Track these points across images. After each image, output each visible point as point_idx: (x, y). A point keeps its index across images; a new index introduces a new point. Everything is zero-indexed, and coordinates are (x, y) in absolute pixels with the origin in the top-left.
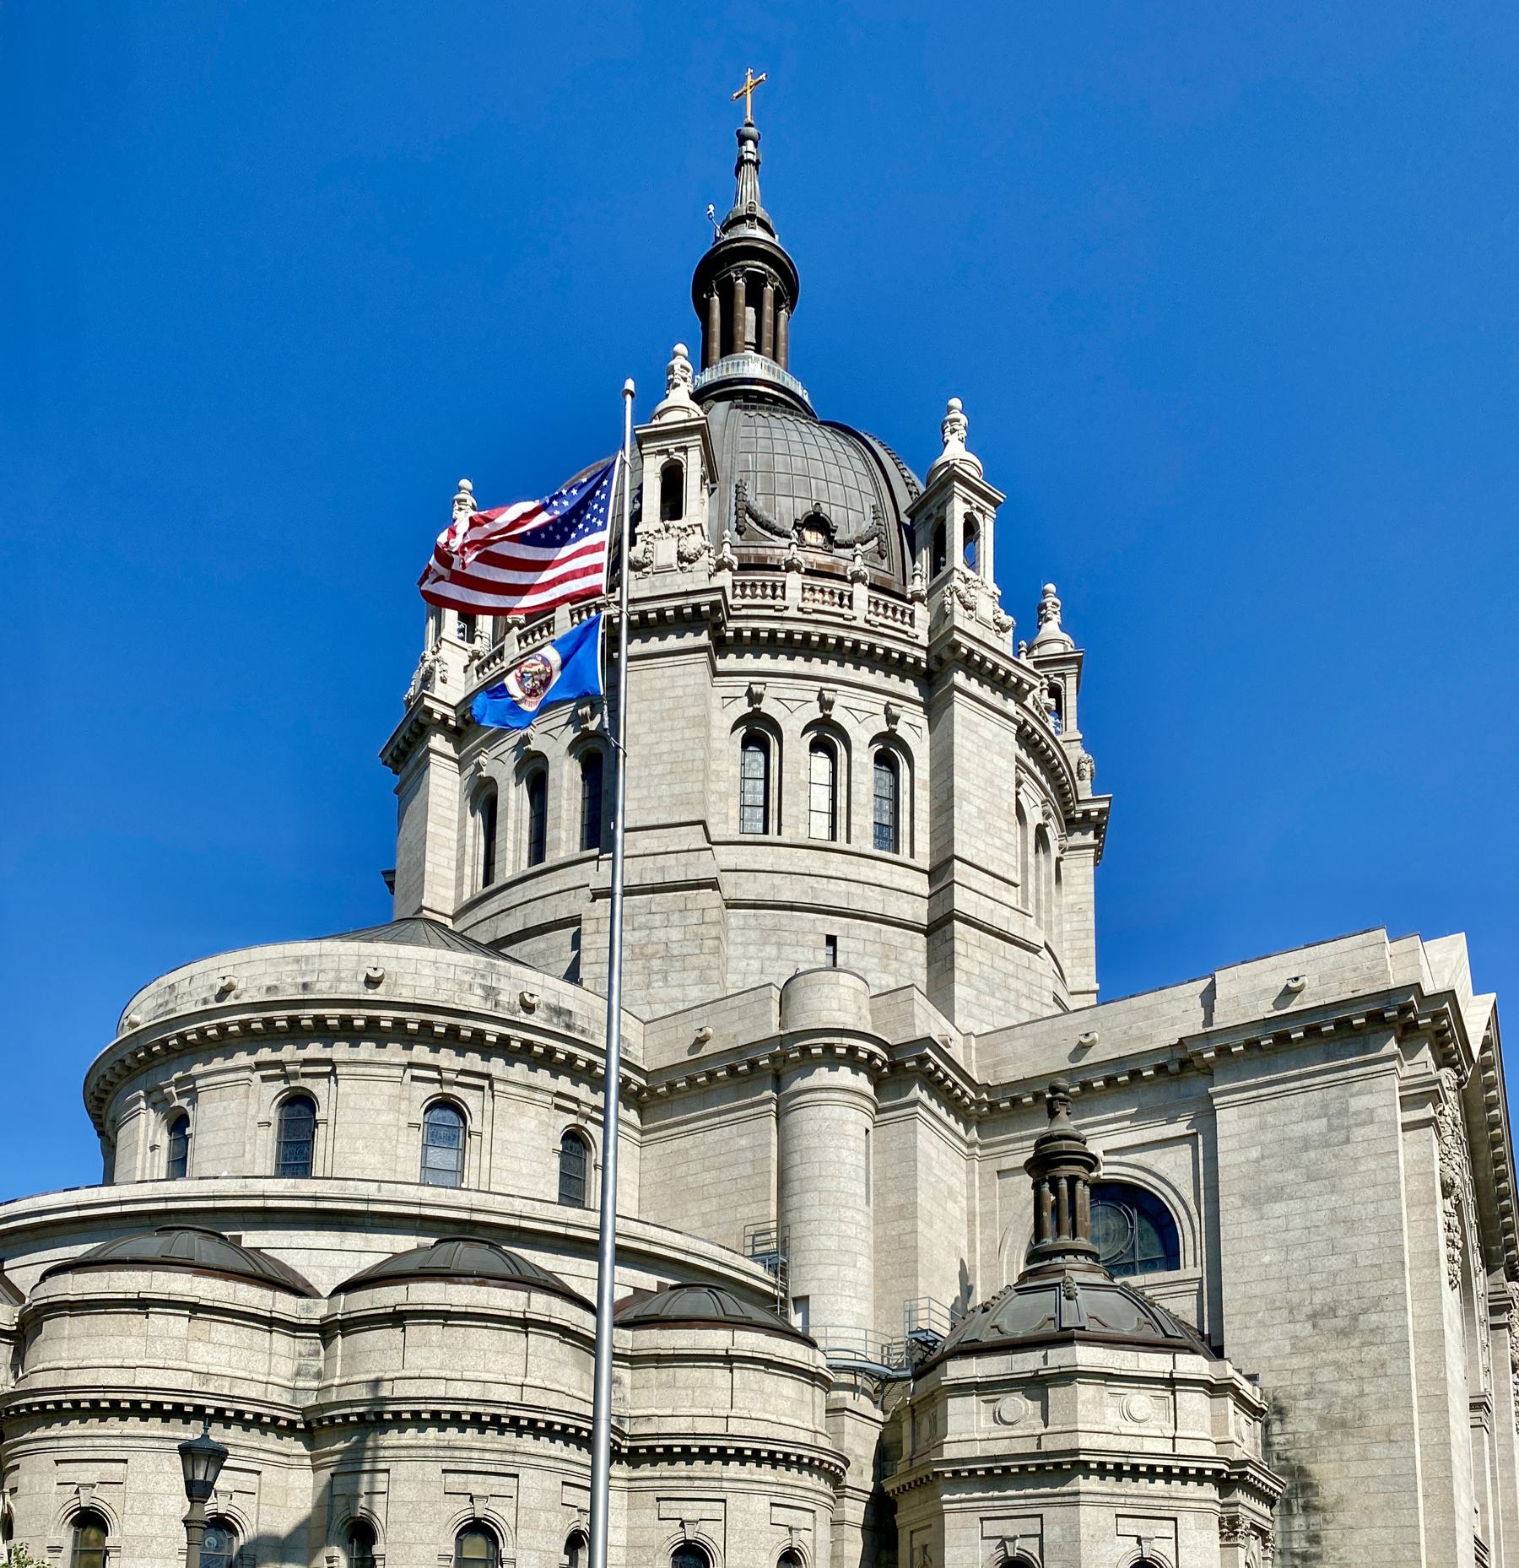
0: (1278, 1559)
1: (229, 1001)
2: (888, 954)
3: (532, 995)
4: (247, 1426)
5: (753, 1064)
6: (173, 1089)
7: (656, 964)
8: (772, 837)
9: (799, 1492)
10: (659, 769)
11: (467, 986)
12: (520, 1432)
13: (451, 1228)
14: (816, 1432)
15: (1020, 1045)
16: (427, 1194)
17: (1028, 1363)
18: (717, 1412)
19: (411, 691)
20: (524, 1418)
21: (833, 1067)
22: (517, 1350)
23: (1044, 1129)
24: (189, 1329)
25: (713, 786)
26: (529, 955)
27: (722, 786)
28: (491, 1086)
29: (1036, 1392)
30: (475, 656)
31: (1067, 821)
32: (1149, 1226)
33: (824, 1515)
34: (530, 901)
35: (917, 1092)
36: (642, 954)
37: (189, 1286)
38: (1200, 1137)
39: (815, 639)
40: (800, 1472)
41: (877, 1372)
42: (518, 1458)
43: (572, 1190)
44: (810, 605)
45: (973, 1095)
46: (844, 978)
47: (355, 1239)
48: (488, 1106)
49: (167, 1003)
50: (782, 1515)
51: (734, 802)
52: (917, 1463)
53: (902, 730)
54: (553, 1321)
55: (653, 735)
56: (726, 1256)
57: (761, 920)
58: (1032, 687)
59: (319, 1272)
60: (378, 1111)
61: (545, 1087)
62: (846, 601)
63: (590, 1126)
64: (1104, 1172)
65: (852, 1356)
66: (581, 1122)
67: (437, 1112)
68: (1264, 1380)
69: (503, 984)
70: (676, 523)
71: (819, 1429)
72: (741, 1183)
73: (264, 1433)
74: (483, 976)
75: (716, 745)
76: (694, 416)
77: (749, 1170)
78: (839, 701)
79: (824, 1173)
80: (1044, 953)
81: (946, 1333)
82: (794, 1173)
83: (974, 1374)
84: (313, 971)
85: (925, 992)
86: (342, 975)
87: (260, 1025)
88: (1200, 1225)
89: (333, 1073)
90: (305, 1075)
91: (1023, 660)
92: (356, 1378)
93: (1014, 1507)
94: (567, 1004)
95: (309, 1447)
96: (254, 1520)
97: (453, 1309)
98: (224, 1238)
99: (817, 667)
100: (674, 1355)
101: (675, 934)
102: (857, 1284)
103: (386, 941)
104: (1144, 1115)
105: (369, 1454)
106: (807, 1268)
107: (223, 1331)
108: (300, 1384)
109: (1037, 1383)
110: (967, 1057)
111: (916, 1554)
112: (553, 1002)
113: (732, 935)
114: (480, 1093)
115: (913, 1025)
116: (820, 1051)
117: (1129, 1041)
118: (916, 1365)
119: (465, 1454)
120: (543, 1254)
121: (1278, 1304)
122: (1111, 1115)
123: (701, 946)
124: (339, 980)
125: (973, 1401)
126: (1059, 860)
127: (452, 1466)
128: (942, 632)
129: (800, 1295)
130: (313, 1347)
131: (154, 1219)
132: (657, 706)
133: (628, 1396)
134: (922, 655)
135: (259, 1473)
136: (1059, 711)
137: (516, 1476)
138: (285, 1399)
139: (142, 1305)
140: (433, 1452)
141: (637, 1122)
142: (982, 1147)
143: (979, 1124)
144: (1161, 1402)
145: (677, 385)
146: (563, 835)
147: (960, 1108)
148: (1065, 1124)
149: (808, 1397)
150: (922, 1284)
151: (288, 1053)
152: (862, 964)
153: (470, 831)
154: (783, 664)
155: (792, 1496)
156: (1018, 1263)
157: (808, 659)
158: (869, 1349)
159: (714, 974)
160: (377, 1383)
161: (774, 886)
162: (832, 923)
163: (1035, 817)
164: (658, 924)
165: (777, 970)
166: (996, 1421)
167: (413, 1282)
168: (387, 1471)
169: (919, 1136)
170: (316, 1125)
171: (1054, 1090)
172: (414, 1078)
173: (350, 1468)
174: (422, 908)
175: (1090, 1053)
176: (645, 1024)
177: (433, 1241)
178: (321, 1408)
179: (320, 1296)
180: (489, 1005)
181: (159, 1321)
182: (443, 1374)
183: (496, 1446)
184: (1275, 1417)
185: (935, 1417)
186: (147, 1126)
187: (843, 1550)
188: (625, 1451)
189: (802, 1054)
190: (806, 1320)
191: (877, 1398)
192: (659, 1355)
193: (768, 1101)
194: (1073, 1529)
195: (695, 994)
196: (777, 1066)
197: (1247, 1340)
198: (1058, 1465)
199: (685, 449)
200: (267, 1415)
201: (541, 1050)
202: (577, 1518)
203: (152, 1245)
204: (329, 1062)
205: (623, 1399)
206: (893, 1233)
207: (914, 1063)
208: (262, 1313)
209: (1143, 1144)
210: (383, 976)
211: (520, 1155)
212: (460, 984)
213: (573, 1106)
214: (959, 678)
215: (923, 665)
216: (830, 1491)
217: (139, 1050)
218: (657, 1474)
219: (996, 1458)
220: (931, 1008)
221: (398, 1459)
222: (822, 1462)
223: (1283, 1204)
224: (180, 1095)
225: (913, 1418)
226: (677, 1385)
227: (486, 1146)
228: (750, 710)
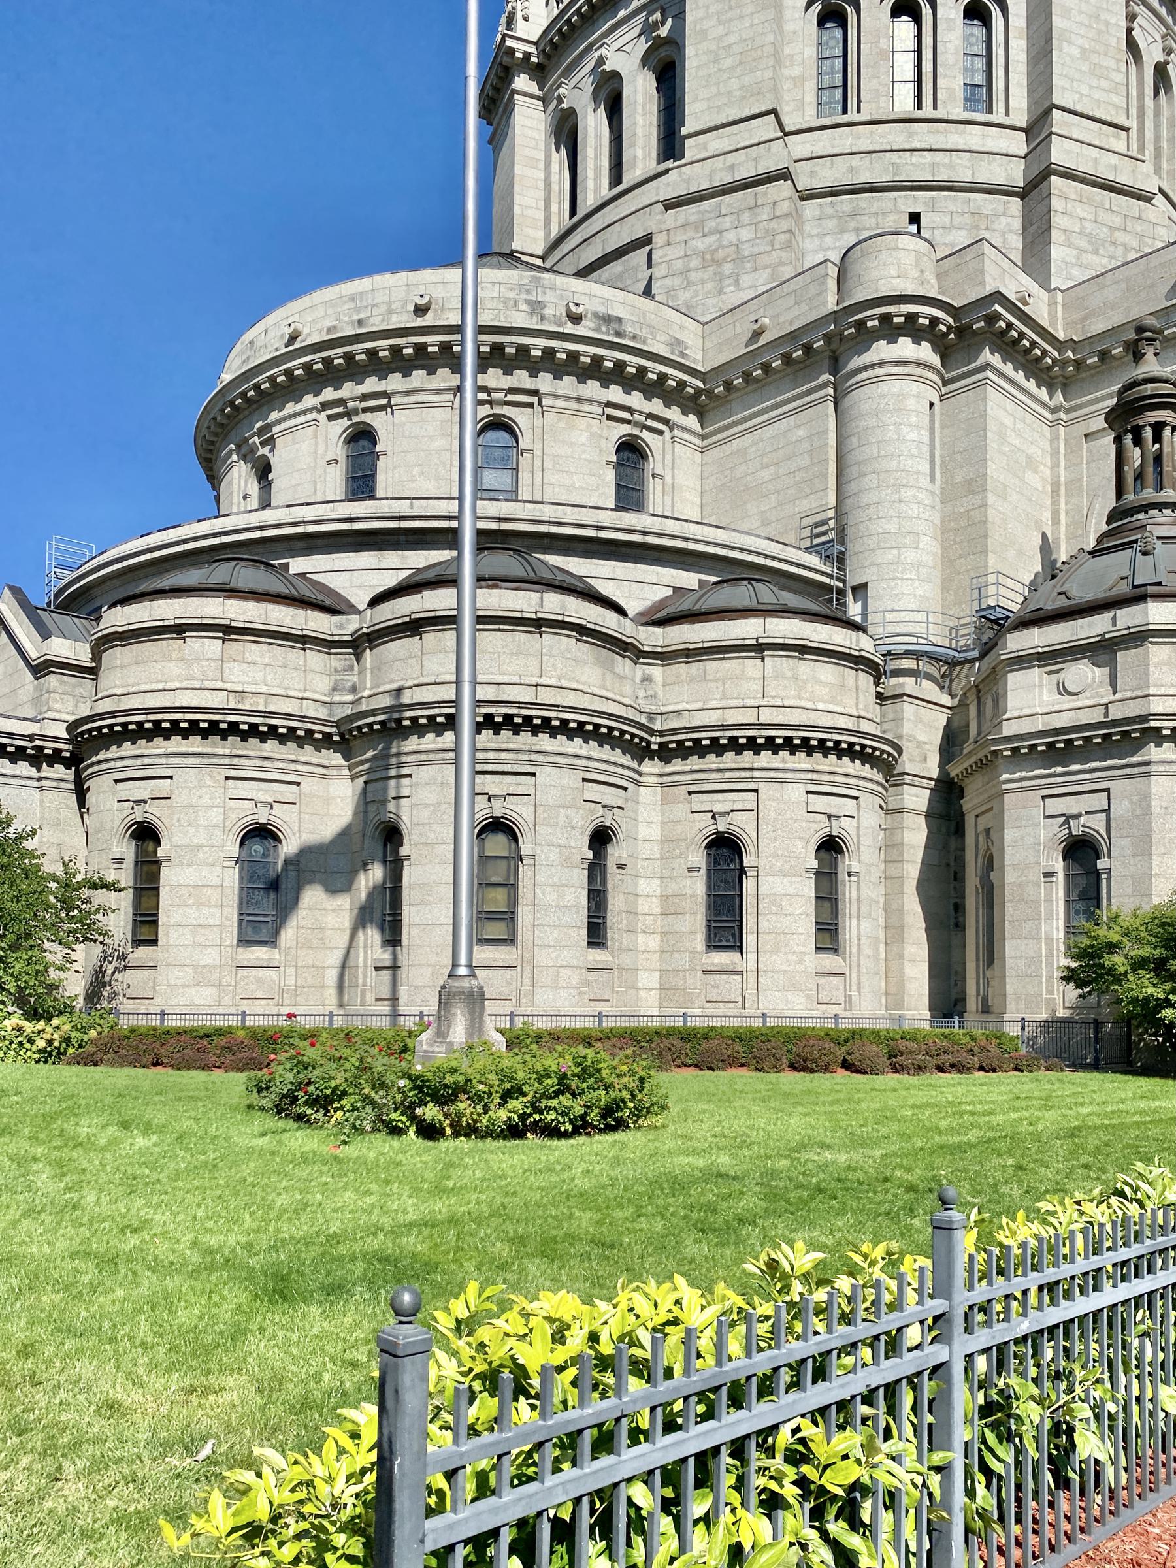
3: (577, 305)
4: (283, 740)
5: (808, 348)
7: (727, 268)
12: (535, 731)
14: (859, 717)
15: (1111, 293)
18: (749, 703)
20: (537, 717)
21: (892, 340)
25: (786, 72)
34: (609, 226)
35: (987, 356)
36: (713, 260)
41: (942, 654)
45: (1056, 354)
50: (819, 803)
51: (811, 86)
55: (721, 27)
56: (774, 549)
66: (636, 432)
72: (799, 476)
73: (301, 746)
75: (789, 27)
77: (805, 461)
79: (882, 453)
80: (1159, 200)
85: (1020, 264)
92: (381, 689)
95: (347, 758)
100: (703, 648)
105: (393, 760)
106: (866, 555)
110: (1053, 317)
115: (983, 283)
116: (876, 322)
118: (986, 644)
120: (576, 559)
123: (772, 244)
125: (1035, 674)
129: (858, 582)
133: (660, 694)
135: (298, 784)
137: (534, 774)
142: (1067, 411)
146: (639, 153)
147: (1041, 370)
153: (555, 167)
158: (931, 631)
160: (399, 690)
164: (728, 225)
166: (1060, 693)
168: (410, 776)
169: (990, 404)
173: (378, 775)
176: (704, 324)
178: (350, 718)
185: (997, 694)
189: (858, 330)
192: (688, 649)
193: (824, 385)
194: (1146, 798)
196: (834, 346)
198: (1126, 734)
200: (301, 729)
201: (588, 360)
202: (601, 814)
205: (654, 696)
206: (962, 510)
211: (572, 470)
213: (626, 415)
216: (879, 777)
218: (687, 768)
219: (1058, 732)
222: (864, 747)
225: (979, 698)
226: (708, 678)
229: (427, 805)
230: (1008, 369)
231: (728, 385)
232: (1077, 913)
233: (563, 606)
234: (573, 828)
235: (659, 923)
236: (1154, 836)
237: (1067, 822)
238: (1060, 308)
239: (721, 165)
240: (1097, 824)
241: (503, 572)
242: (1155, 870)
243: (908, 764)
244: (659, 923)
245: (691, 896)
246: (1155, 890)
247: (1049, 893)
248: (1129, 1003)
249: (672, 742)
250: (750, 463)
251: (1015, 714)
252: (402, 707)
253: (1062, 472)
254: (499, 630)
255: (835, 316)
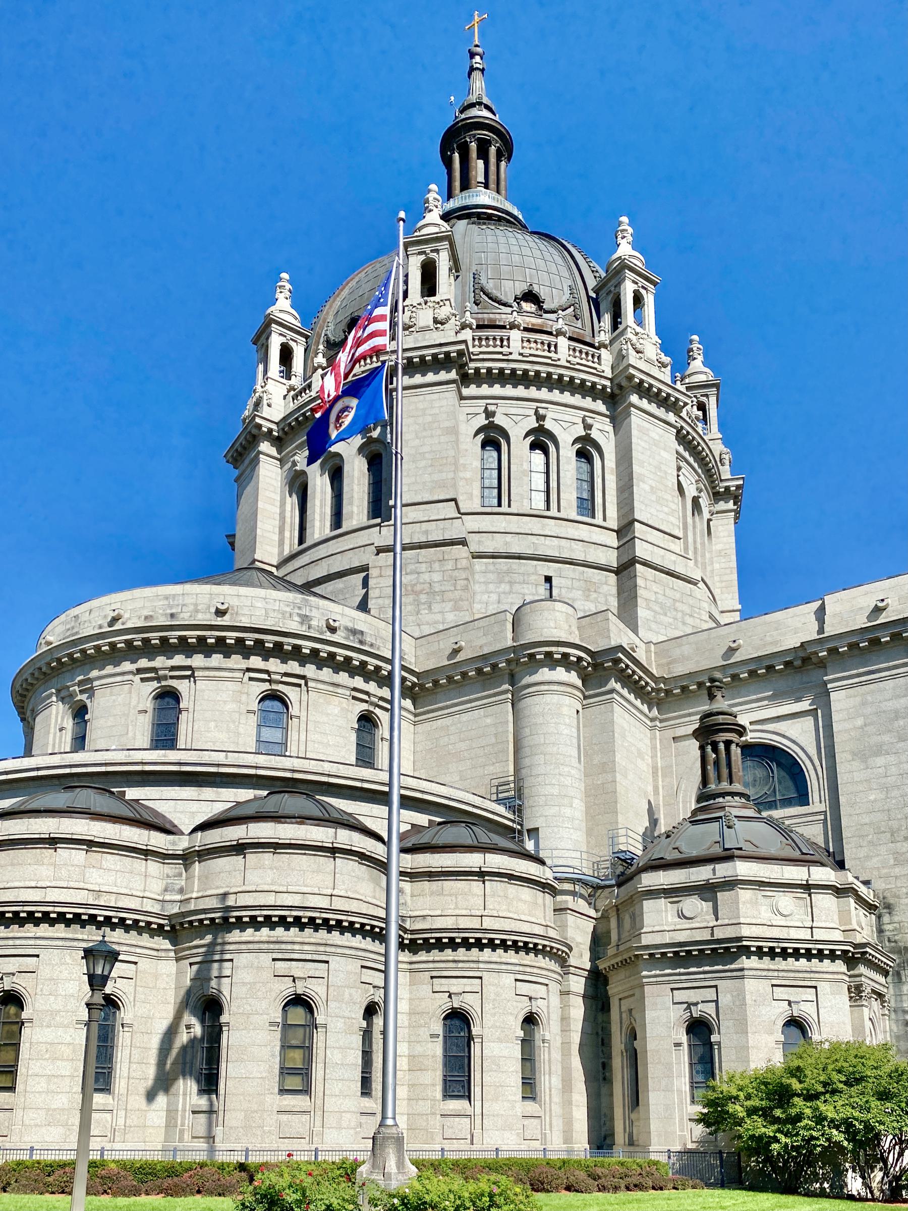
0: (893, 1016)
1: (118, 626)
2: (589, 589)
5: (494, 666)
6: (76, 688)
7: (423, 598)
8: (504, 508)
9: (535, 970)
10: (423, 463)
11: (288, 615)
13: (279, 783)
14: (547, 926)
16: (262, 760)
17: (701, 874)
19: (247, 413)
20: (333, 919)
21: (553, 668)
22: (328, 870)
23: (706, 708)
24: (86, 859)
25: (461, 475)
26: (332, 592)
27: (468, 475)
28: (306, 684)
29: (708, 895)
30: (291, 388)
31: (714, 494)
32: (785, 774)
33: (554, 987)
36: (413, 591)
37: (86, 828)
38: (819, 711)
39: (532, 374)
40: (536, 956)
42: (328, 949)
43: (365, 757)
44: (527, 351)
45: (653, 685)
46: (558, 605)
47: (208, 793)
48: (304, 697)
49: (73, 628)
50: (524, 988)
51: (477, 486)
52: (622, 948)
53: (595, 434)
54: (354, 848)
56: (477, 801)
57: (497, 566)
58: (686, 404)
59: (182, 816)
60: (225, 702)
61: (345, 684)
62: (553, 348)
63: (377, 711)
64: (750, 737)
65: (571, 870)
66: (371, 708)
67: (268, 703)
68: (875, 884)
69: (314, 613)
70: (432, 299)
71: (549, 924)
74: (300, 608)
76: (443, 229)
78: (550, 415)
79: (547, 742)
81: (640, 853)
82: (526, 742)
83: (662, 882)
84: (178, 605)
86: (199, 608)
87: (140, 643)
88: (823, 774)
89: (193, 675)
90: (172, 677)
91: (678, 386)
93: (696, 980)
94: (359, 627)
96: (132, 999)
97: (280, 842)
98: (113, 793)
99: (533, 392)
101: (436, 577)
102: (573, 819)
103: (230, 584)
104: (778, 697)
105: (218, 948)
107: (111, 860)
108: (168, 898)
109: (708, 889)
110: (648, 659)
111: (624, 1015)
112: (350, 625)
113: (477, 577)
114: (298, 689)
115: (609, 637)
116: (542, 656)
117: (764, 645)
118: (619, 876)
119: (289, 947)
120: (345, 801)
121: (883, 829)
122: (754, 697)
123: (455, 585)
124: (197, 611)
125: (662, 902)
126: (709, 520)
127: (280, 956)
128: (621, 368)
129: (532, 827)
130: (177, 871)
131: (62, 780)
132: (420, 420)
134: (608, 383)
136: (705, 420)
137: (327, 962)
138: (156, 908)
139: (53, 842)
140: (265, 946)
141: (411, 708)
142: (661, 721)
143: (658, 705)
144: (801, 902)
145: (431, 211)
148: (721, 704)
149: (540, 901)
150: (620, 818)
151: (160, 662)
152: (571, 595)
154: (509, 391)
155: (531, 974)
156: (690, 802)
157: (527, 388)
159: (465, 604)
160: (225, 895)
161: (506, 543)
162: (549, 568)
163: (691, 491)
164: (424, 570)
165: (510, 600)
166: (679, 917)
167: (251, 822)
168: (231, 960)
169: (615, 715)
170: (180, 712)
171: (712, 680)
172: (251, 679)
174: (254, 561)
175: (738, 653)
176: (416, 639)
177: (265, 793)
178: (183, 914)
179: (183, 834)
180: (304, 628)
181: (64, 854)
182: (273, 888)
183: (312, 940)
184: (885, 911)
185: (634, 914)
186: (57, 713)
187: (569, 1014)
188: (407, 942)
189: (530, 659)
190: (537, 845)
191: (590, 899)
193: (506, 692)
195: (451, 618)
196: (512, 667)
197: (862, 856)
198: (727, 949)
199: (437, 251)
202: (372, 992)
203: (60, 799)
204: (189, 668)
205: (405, 904)
207: (610, 664)
208: (140, 847)
209: (778, 717)
210: (228, 608)
212: (283, 613)
214: (634, 398)
215: (609, 390)
216: (559, 970)
217: (52, 660)
218: (431, 959)
219: (681, 944)
220: (622, 625)
221: (240, 952)
222: (552, 948)
223: (883, 758)
224: (81, 692)
225: (618, 915)
226: (445, 893)
227: (303, 726)
228: (487, 422)
229: (244, 984)
230: (625, 692)
231: (436, 683)
232: (697, 1072)
233: (350, 838)
234: (354, 1003)
235: (407, 1077)
236: (749, 1019)
237: (689, 1007)
238: (653, 655)
239: (418, 530)
240: (710, 1009)
241: (306, 813)
242: (751, 1043)
243: (572, 961)
244: (407, 1077)
245: (433, 1057)
246: (752, 1058)
247: (678, 1058)
248: (748, 1139)
249: (420, 939)
250: (451, 737)
251: (650, 930)
252: (229, 909)
253: (659, 760)
254: (305, 854)
255: (514, 649)
